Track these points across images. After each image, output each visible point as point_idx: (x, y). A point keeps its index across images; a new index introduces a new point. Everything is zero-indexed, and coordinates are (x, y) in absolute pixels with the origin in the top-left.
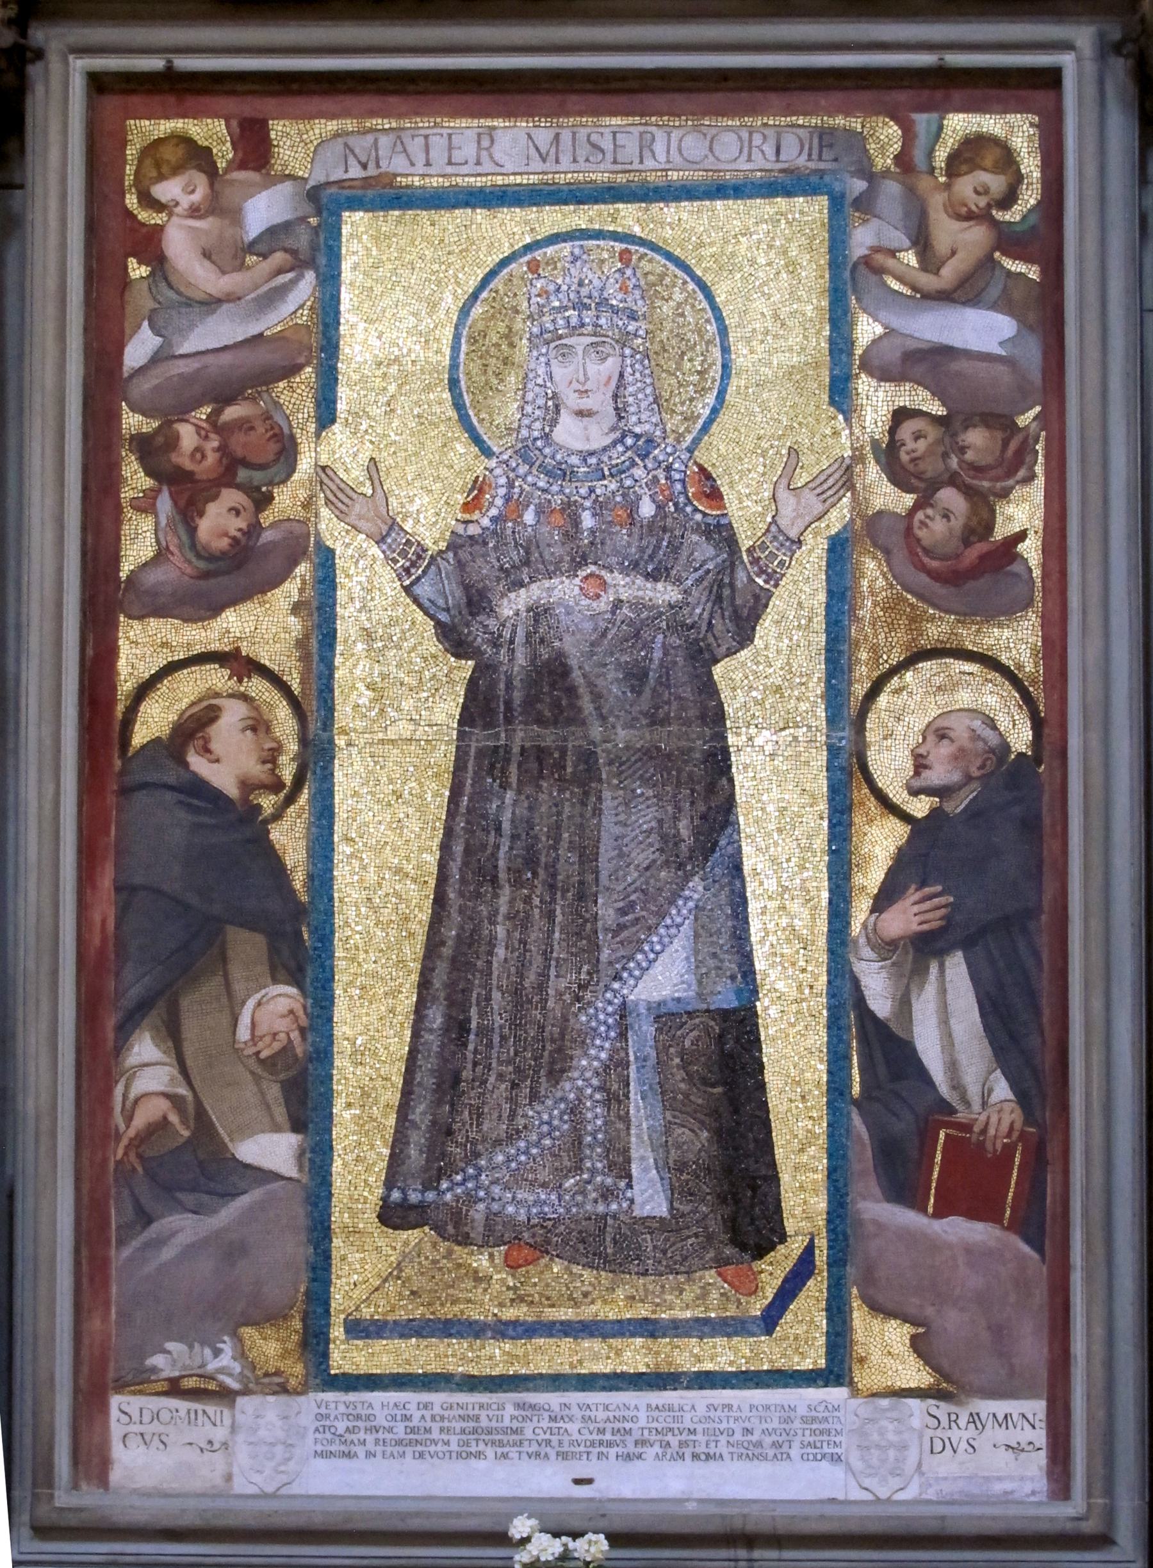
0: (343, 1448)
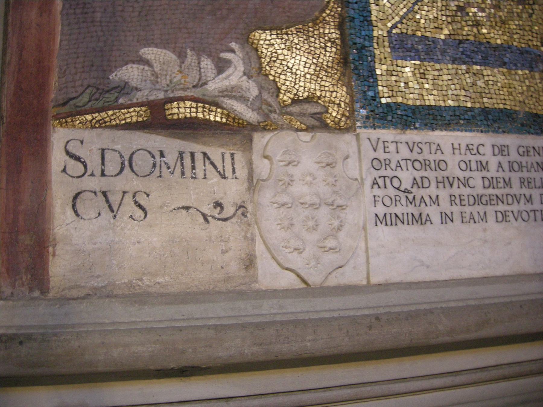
0: (411, 209)
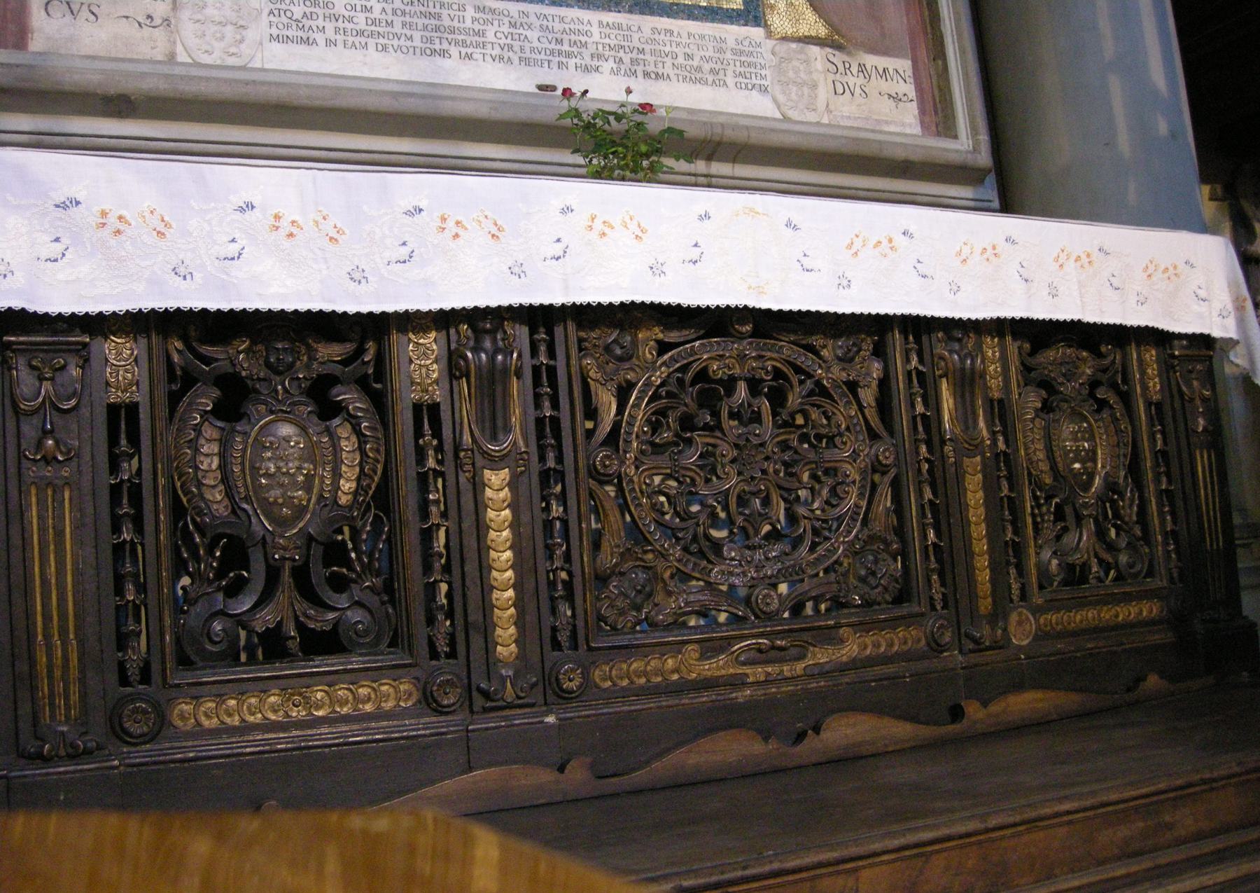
0: (300, 33)
